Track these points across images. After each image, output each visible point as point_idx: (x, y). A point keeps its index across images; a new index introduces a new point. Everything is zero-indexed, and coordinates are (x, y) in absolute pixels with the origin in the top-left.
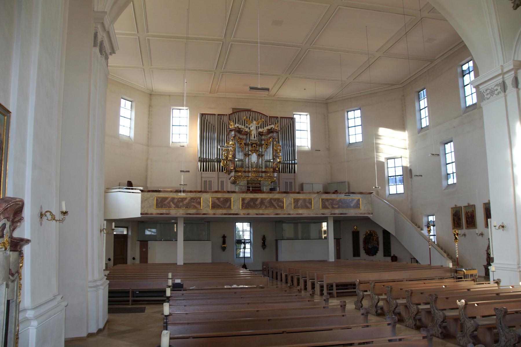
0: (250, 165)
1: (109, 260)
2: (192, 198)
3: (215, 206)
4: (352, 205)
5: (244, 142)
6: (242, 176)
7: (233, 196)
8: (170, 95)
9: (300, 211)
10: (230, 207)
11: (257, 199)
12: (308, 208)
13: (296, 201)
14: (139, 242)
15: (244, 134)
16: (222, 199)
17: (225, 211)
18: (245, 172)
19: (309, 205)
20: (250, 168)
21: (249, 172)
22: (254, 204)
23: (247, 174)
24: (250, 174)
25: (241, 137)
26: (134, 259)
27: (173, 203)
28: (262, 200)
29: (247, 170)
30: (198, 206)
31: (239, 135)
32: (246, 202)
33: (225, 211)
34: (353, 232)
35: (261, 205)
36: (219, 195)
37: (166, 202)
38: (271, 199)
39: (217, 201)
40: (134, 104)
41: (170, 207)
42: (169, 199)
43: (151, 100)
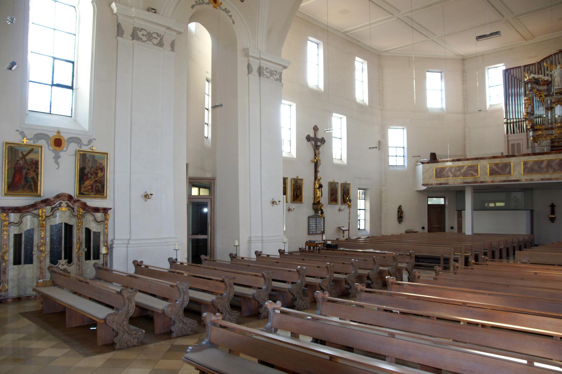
0: (554, 120)
1: (423, 228)
2: (470, 167)
3: (493, 173)
5: (546, 93)
6: (543, 135)
7: (512, 160)
8: (483, 55)
10: (509, 173)
11: (542, 162)
15: (544, 85)
16: (500, 165)
17: (503, 178)
18: (546, 129)
20: (554, 124)
21: (552, 129)
22: (539, 167)
23: (550, 132)
24: (554, 132)
25: (541, 88)
26: (452, 228)
27: (451, 172)
28: (549, 162)
29: (550, 126)
30: (474, 174)
31: (538, 87)
32: (529, 166)
33: (503, 178)
35: (548, 169)
36: (497, 161)
37: (444, 172)
39: (495, 167)
40: (443, 74)
41: (448, 177)
42: (447, 168)
43: (464, 64)
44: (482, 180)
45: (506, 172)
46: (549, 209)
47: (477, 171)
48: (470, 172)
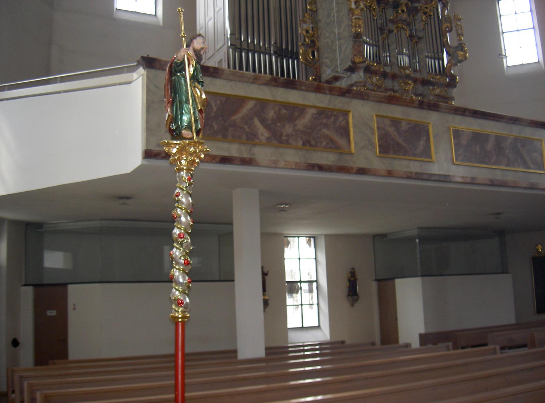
2: (322, 112)
10: (427, 153)
14: (30, 289)
23: (389, 83)
24: (396, 84)
26: (15, 343)
27: (263, 122)
30: (341, 141)
37: (237, 117)
38: (516, 139)
39: (391, 130)
44: (360, 163)
45: (418, 151)
47: (345, 132)
48: (325, 131)
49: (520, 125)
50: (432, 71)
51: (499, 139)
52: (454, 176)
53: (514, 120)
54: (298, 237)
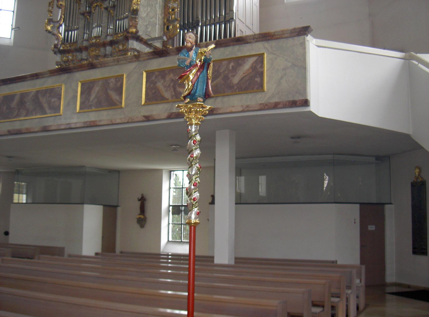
4: (236, 80)
9: (92, 117)
12: (113, 104)
13: (87, 88)
19: (114, 96)
23: (84, 55)
34: (413, 185)
38: (38, 92)
46: (138, 204)
49: (43, 77)
50: (118, 31)
51: (23, 96)
52: (50, 126)
53: (36, 76)
54: (183, 171)
